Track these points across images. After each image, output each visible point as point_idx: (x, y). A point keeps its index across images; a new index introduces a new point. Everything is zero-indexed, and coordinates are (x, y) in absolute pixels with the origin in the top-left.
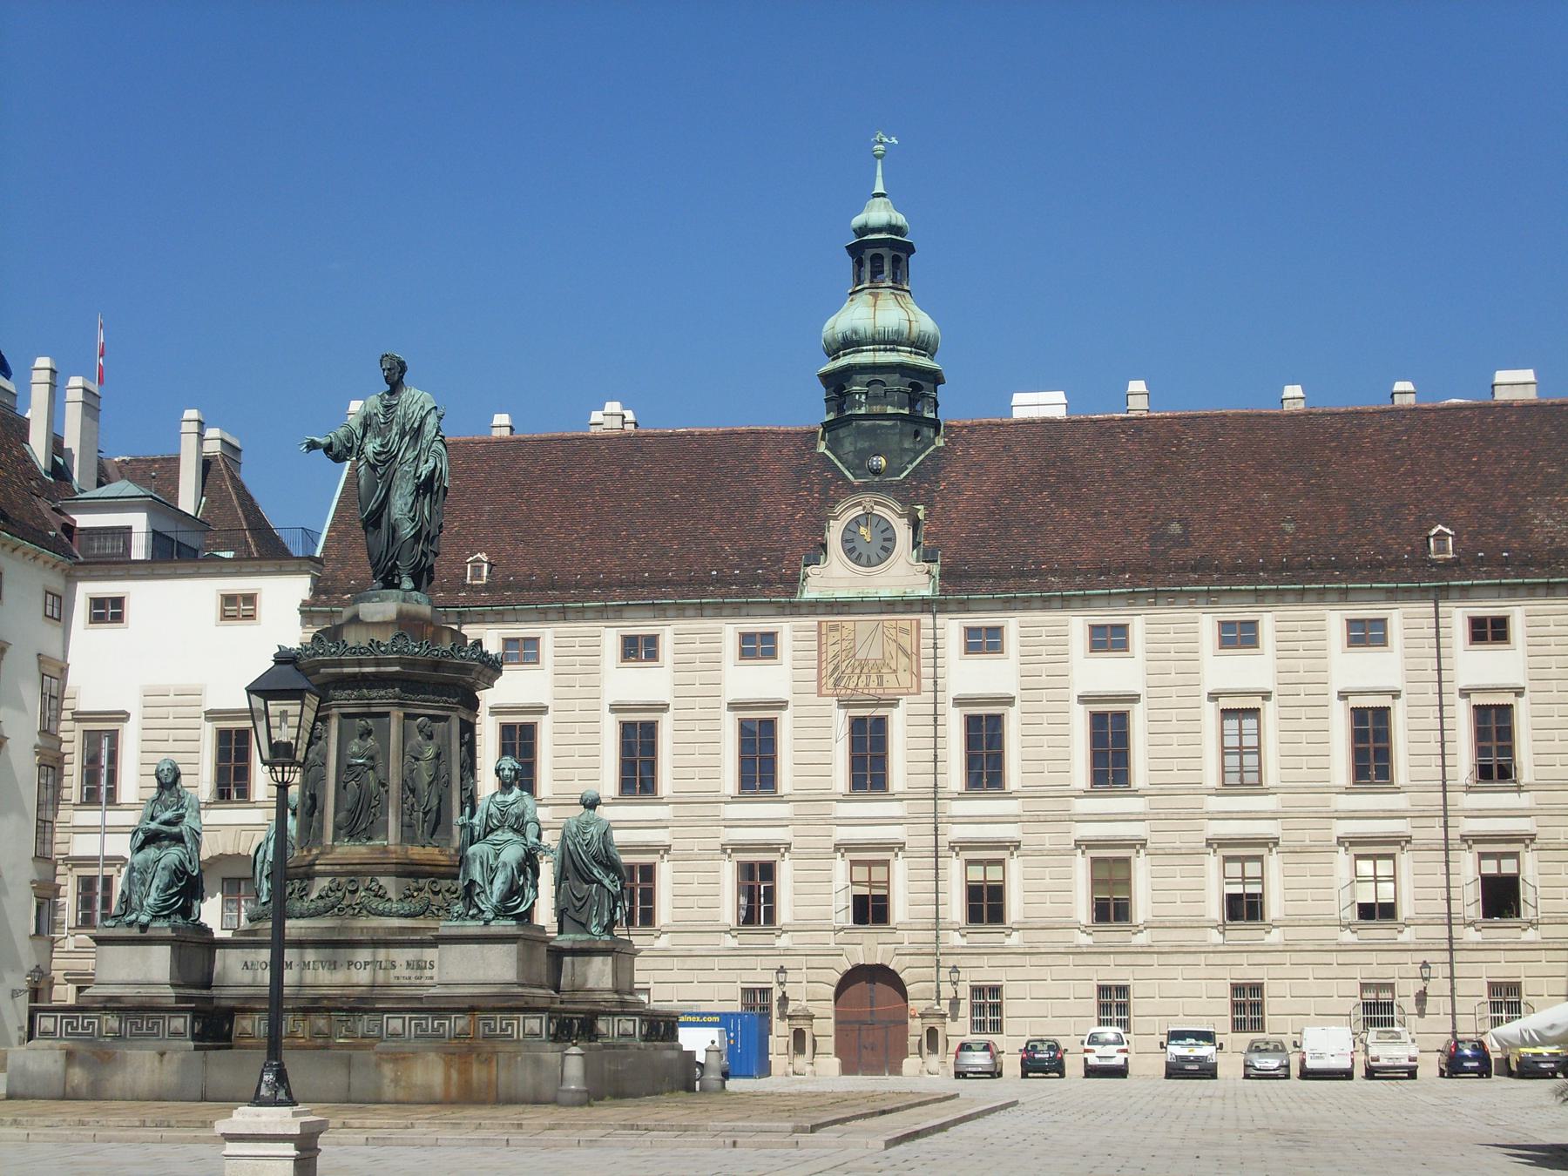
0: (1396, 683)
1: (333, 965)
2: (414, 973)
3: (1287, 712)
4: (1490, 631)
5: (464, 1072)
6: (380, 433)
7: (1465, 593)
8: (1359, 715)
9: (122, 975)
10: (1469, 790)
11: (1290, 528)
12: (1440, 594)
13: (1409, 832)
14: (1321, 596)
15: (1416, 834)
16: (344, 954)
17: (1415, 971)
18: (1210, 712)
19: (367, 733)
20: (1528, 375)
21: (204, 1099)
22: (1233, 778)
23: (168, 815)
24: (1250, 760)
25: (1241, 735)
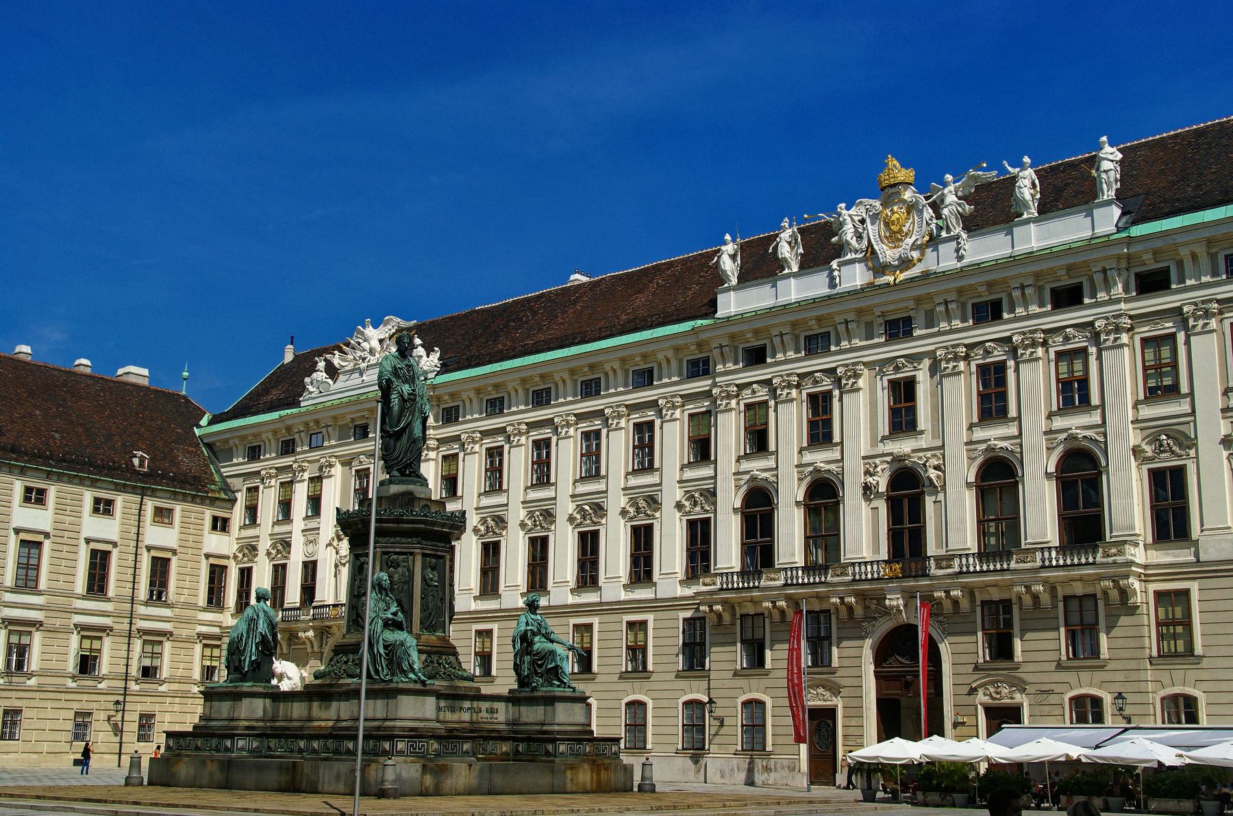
0: (115, 538)
1: (453, 710)
2: (489, 716)
3: (57, 547)
4: (163, 515)
5: (599, 775)
6: (406, 381)
7: (153, 493)
8: (94, 553)
9: (411, 714)
10: (146, 604)
11: (57, 436)
12: (143, 493)
13: (111, 624)
14: (81, 482)
15: (116, 626)
16: (458, 703)
17: (111, 706)
18: (13, 543)
19: (433, 569)
20: (145, 372)
21: (489, 794)
22: (21, 583)
23: (393, 609)
24: (32, 573)
25: (29, 558)
